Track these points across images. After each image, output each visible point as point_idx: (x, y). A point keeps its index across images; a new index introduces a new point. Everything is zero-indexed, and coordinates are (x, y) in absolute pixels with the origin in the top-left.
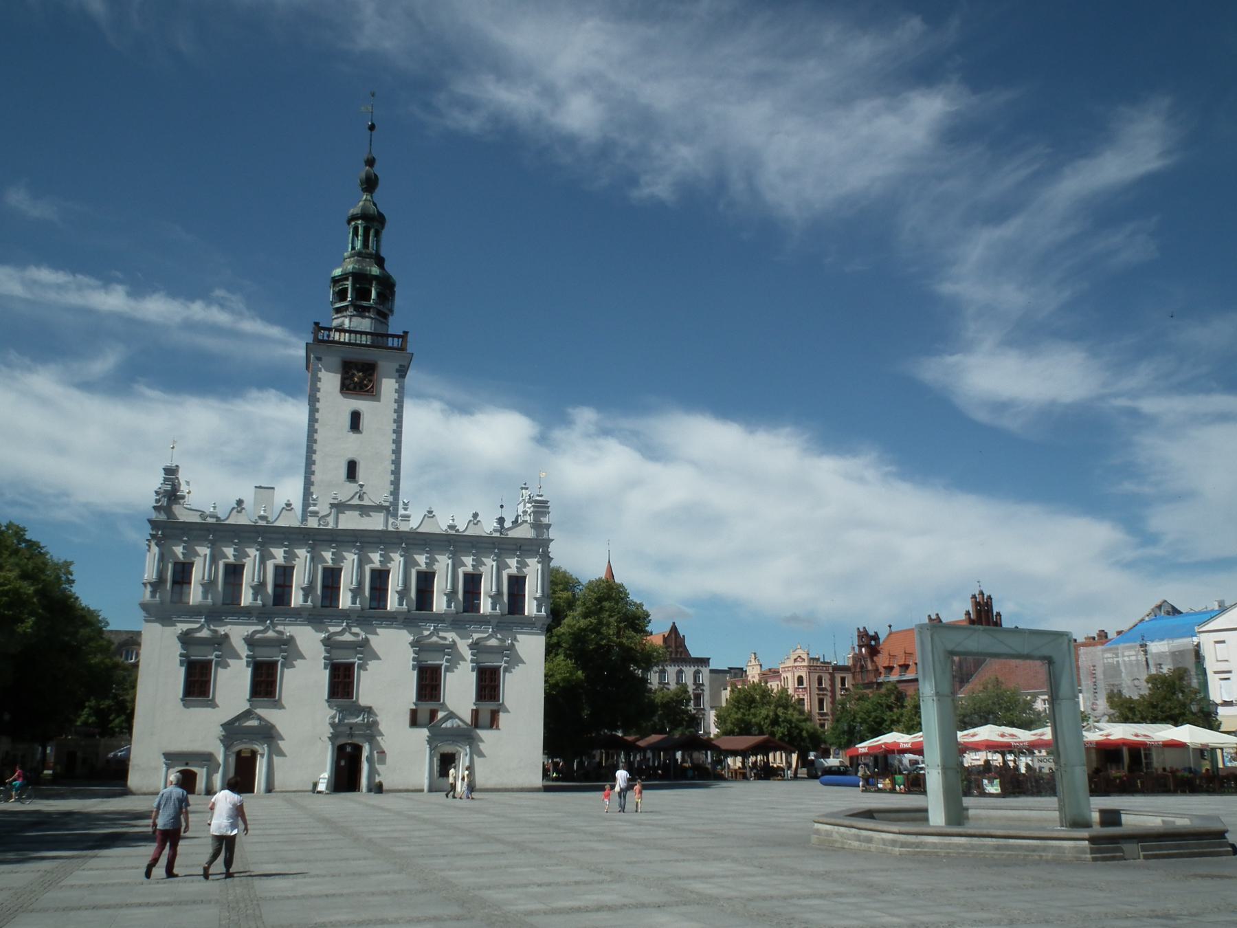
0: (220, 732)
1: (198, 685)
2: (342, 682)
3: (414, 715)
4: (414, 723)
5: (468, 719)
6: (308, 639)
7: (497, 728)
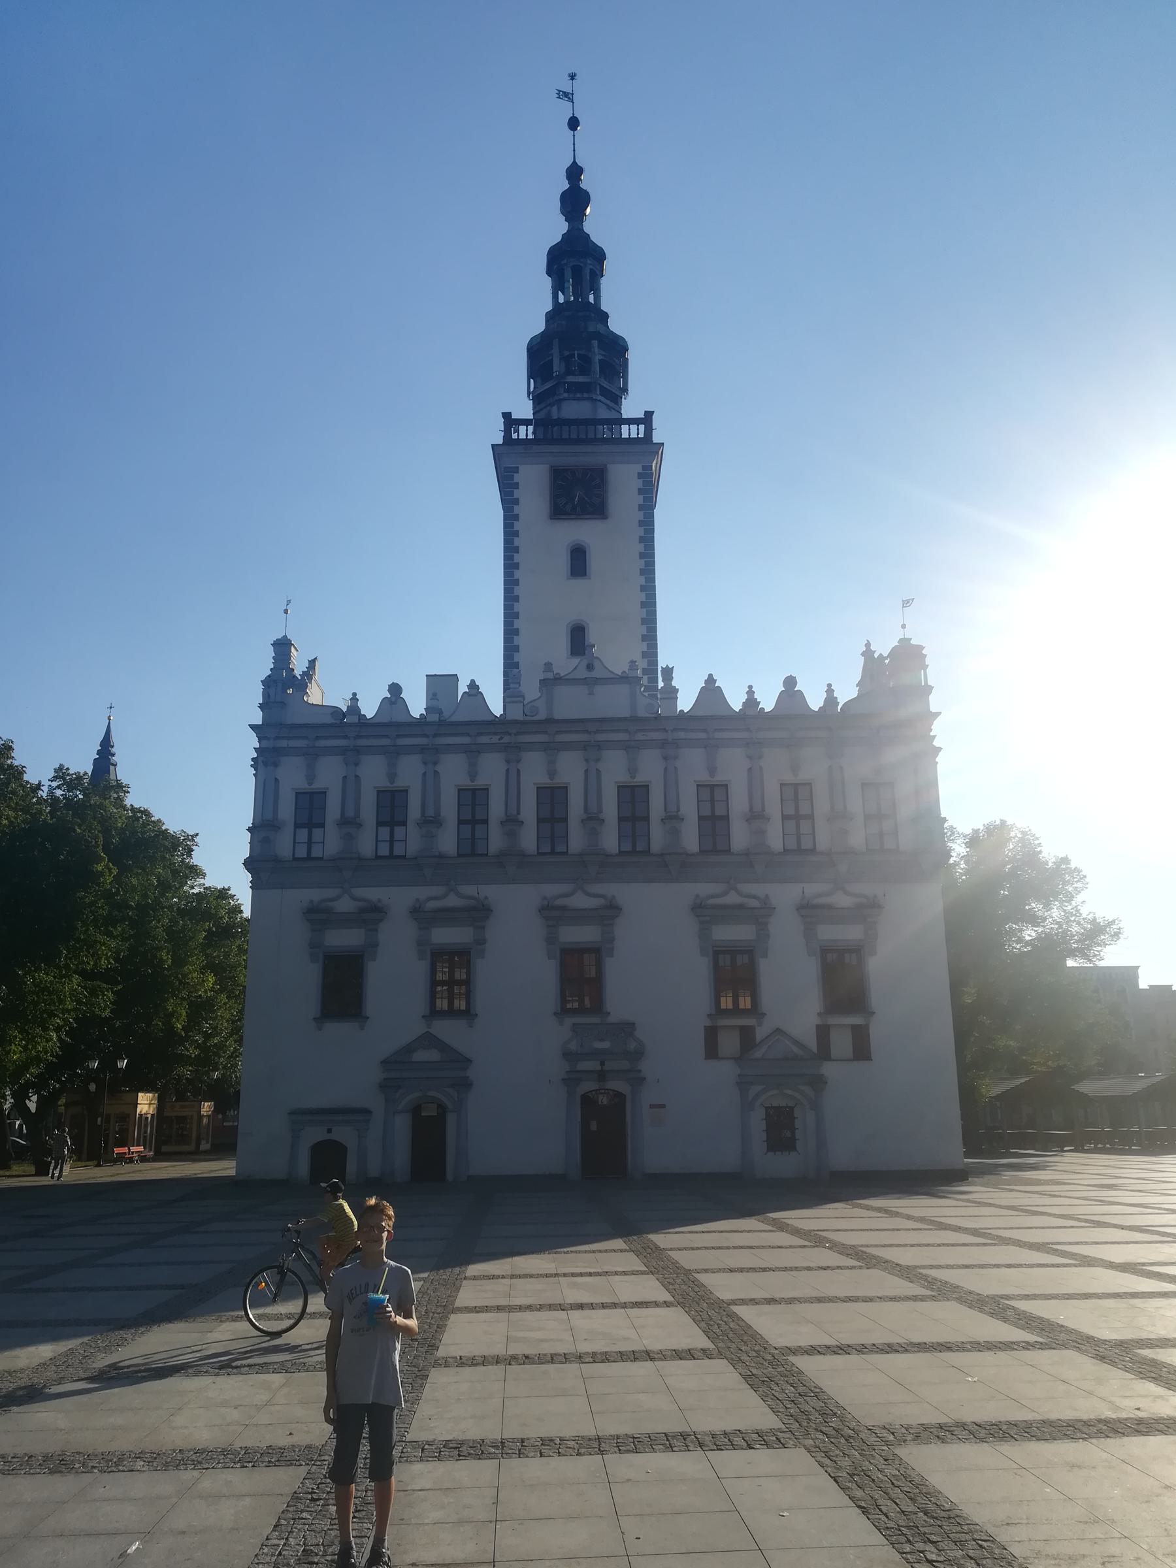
1: (342, 988)
2: (580, 978)
3: (711, 1034)
4: (712, 1051)
5: (813, 1045)
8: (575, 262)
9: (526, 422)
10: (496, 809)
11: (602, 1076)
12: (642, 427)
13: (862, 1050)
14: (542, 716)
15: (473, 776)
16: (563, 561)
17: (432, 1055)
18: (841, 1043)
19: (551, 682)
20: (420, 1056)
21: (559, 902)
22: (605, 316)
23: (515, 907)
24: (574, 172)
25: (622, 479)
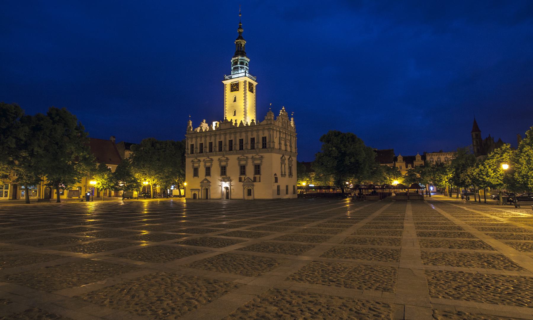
0: (200, 184)
5: (252, 179)
18: (258, 179)
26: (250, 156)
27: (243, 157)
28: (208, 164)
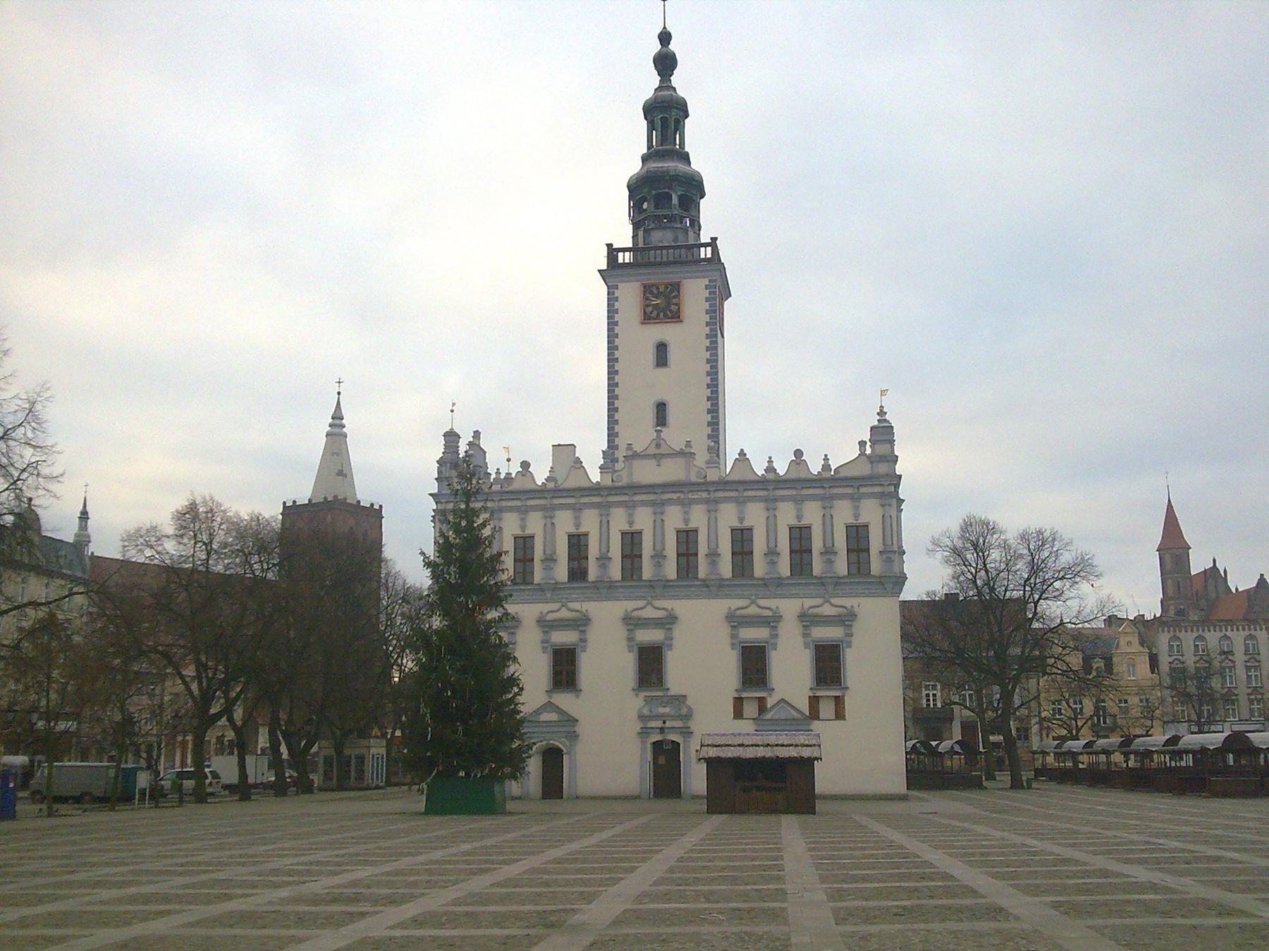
2: (650, 665)
3: (738, 702)
4: (738, 714)
5: (806, 709)
6: (607, 616)
7: (843, 718)
8: (666, 115)
9: (624, 250)
10: (593, 550)
11: (662, 730)
12: (709, 249)
13: (840, 715)
14: (625, 481)
15: (578, 525)
16: (650, 356)
17: (553, 717)
18: (827, 709)
19: (633, 456)
20: (545, 717)
21: (636, 614)
22: (685, 158)
23: (607, 616)
24: (665, 37)
25: (694, 292)
26: (789, 607)
27: (753, 610)
28: (564, 638)
